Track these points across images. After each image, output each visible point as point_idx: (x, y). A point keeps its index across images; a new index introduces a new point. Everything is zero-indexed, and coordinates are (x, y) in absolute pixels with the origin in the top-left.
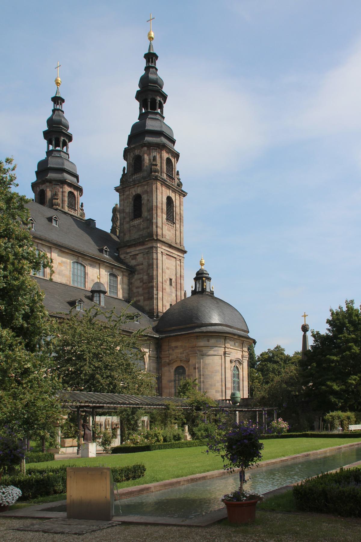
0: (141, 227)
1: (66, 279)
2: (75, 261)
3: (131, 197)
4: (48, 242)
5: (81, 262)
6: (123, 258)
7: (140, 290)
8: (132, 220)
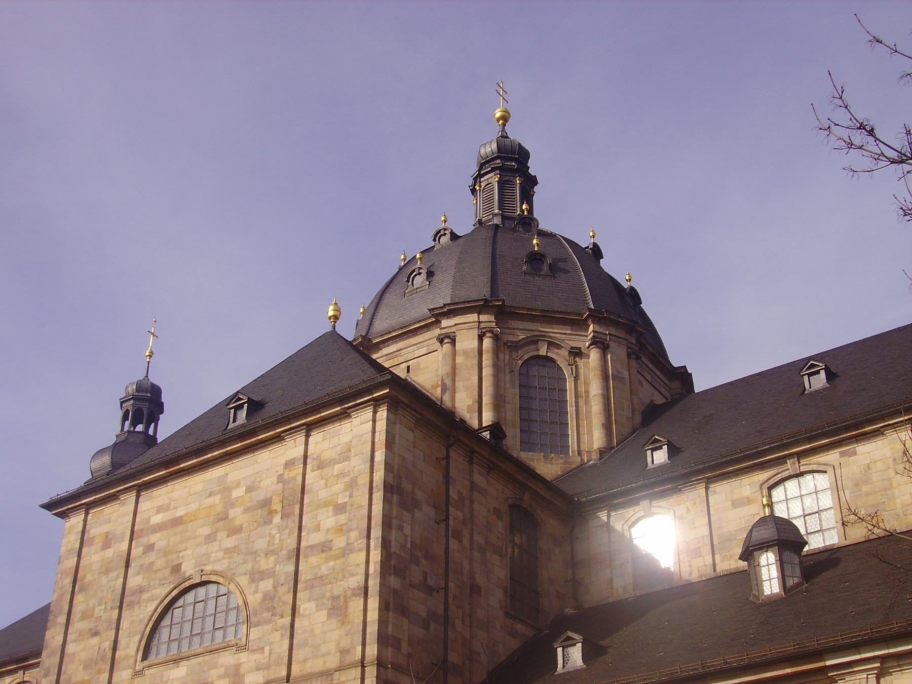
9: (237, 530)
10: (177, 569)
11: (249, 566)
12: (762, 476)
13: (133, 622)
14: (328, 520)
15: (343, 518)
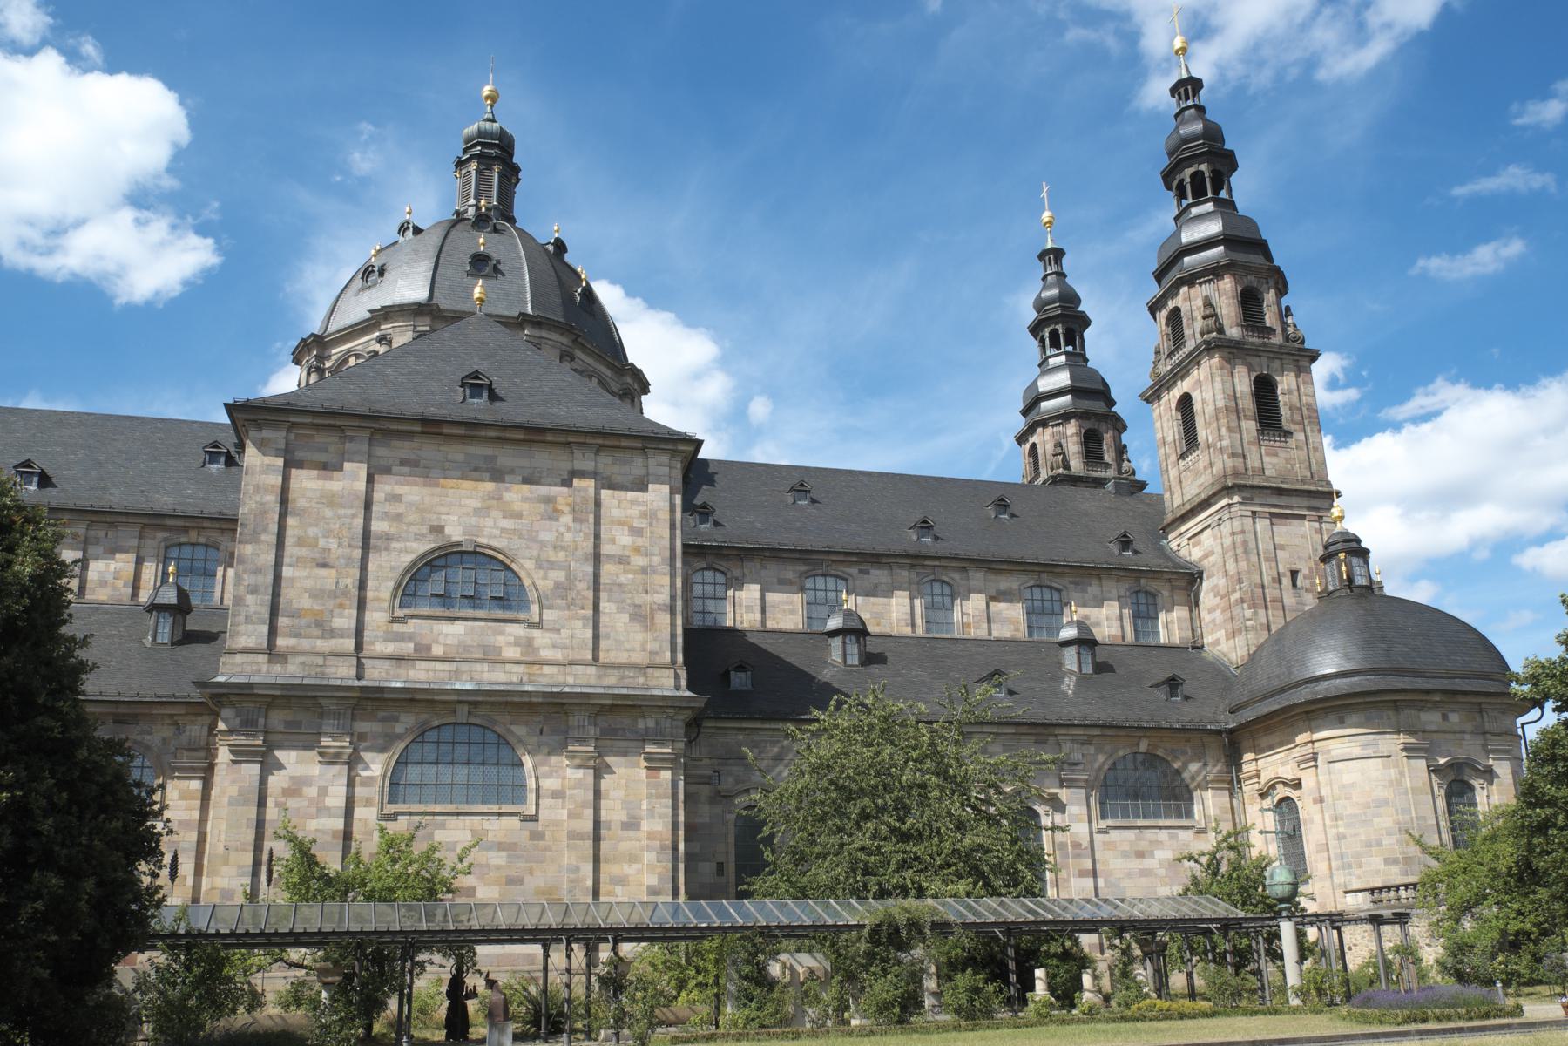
0: (1201, 465)
1: (1012, 627)
2: (1032, 583)
3: (1173, 406)
4: (955, 558)
5: (1049, 583)
6: (1176, 548)
7: (1217, 614)
8: (1182, 456)
9: (519, 516)
10: (438, 530)
11: (535, 553)
12: (803, 568)
13: (380, 567)
14: (625, 539)
15: (640, 541)
